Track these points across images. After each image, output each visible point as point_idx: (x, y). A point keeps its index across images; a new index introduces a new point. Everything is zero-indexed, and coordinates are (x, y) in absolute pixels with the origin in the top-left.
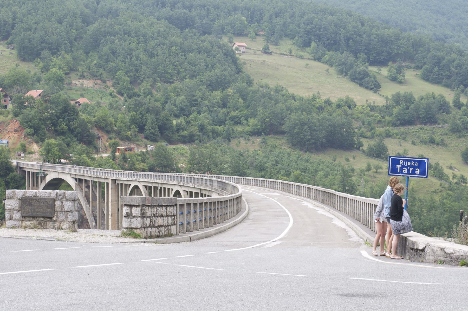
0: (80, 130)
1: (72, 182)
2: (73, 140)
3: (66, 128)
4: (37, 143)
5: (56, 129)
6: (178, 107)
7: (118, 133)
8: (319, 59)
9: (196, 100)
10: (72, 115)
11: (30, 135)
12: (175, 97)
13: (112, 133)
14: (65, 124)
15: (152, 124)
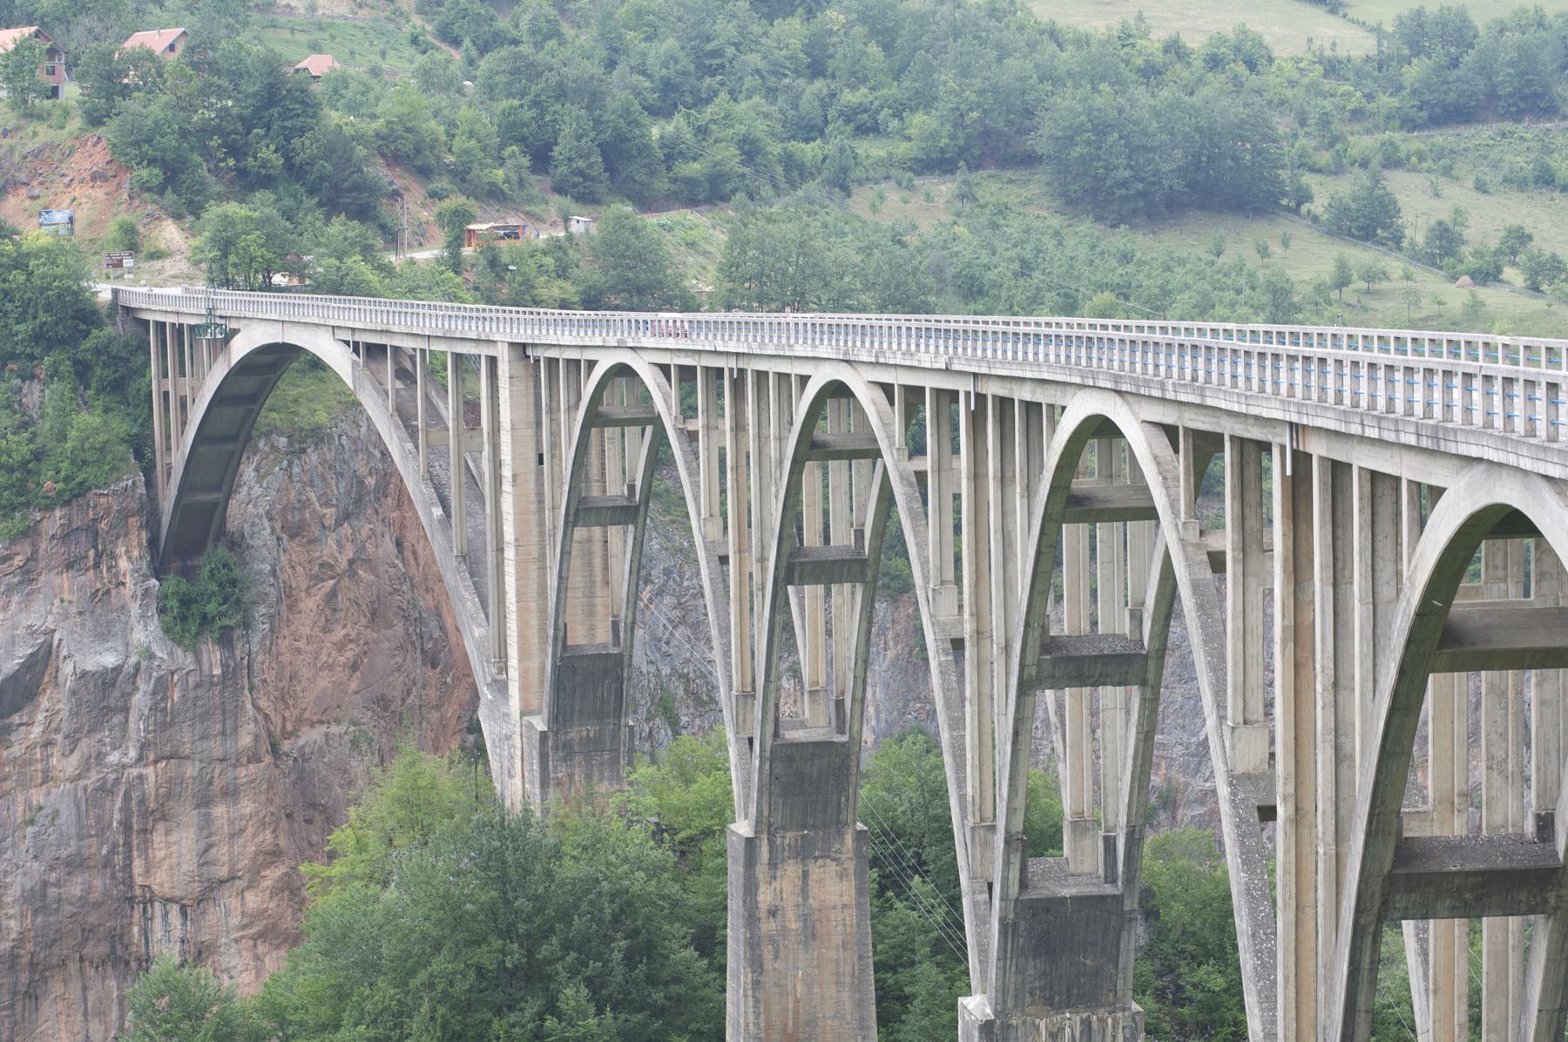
0: (329, 168)
1: (339, 359)
2: (304, 206)
3: (277, 160)
4: (177, 217)
5: (242, 165)
6: (657, 77)
7: (461, 176)
9: (717, 53)
10: (298, 116)
11: (149, 190)
12: (643, 44)
13: (440, 174)
14: (273, 147)
15: (579, 138)
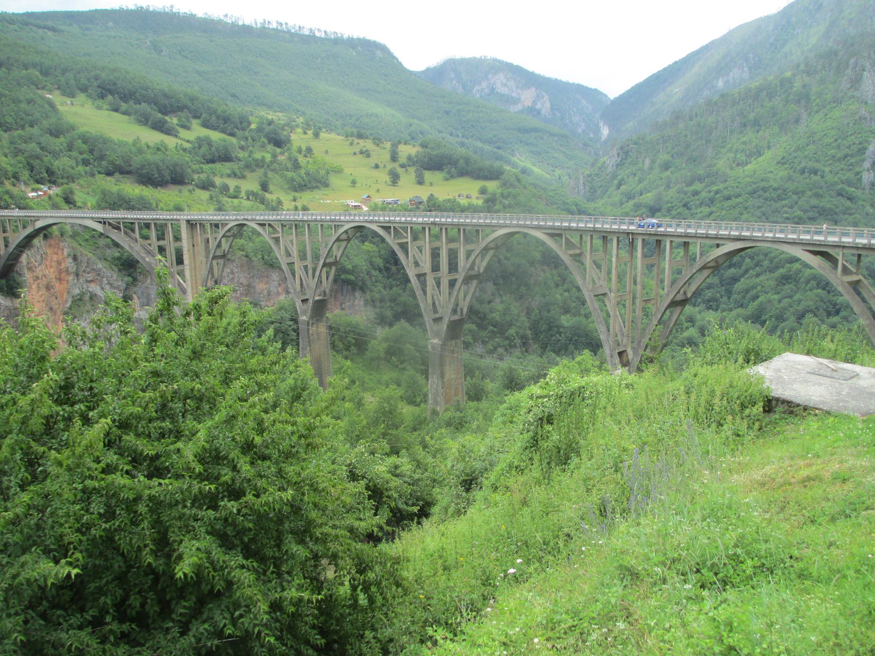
8: (116, 110)
